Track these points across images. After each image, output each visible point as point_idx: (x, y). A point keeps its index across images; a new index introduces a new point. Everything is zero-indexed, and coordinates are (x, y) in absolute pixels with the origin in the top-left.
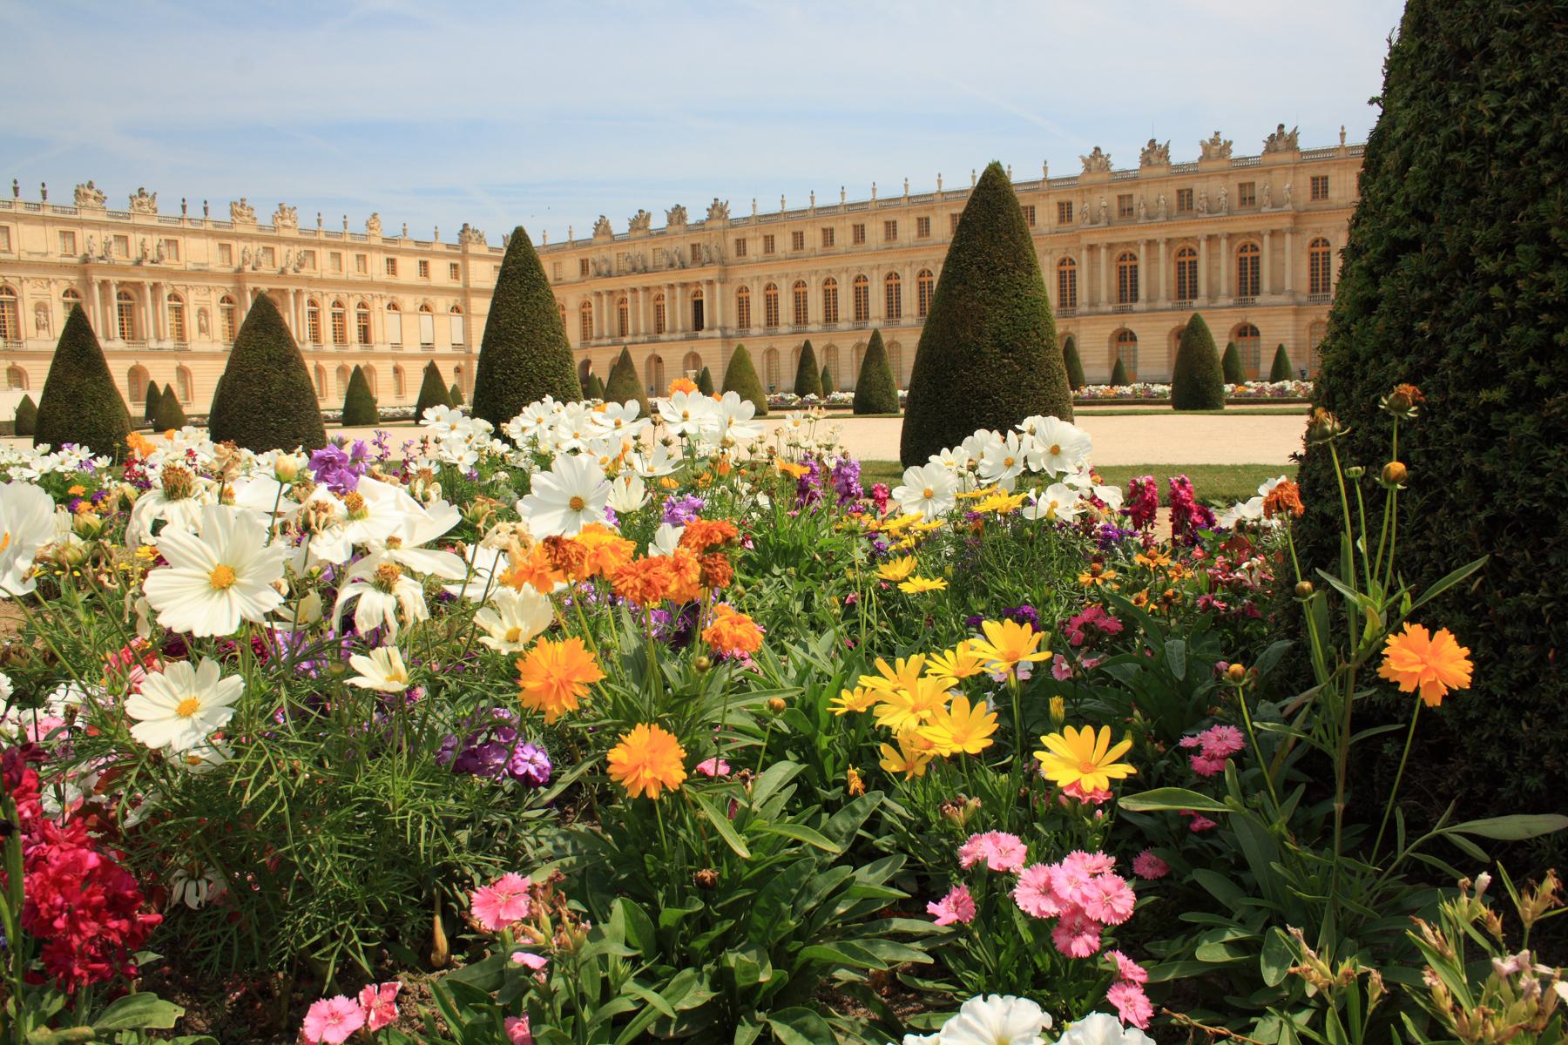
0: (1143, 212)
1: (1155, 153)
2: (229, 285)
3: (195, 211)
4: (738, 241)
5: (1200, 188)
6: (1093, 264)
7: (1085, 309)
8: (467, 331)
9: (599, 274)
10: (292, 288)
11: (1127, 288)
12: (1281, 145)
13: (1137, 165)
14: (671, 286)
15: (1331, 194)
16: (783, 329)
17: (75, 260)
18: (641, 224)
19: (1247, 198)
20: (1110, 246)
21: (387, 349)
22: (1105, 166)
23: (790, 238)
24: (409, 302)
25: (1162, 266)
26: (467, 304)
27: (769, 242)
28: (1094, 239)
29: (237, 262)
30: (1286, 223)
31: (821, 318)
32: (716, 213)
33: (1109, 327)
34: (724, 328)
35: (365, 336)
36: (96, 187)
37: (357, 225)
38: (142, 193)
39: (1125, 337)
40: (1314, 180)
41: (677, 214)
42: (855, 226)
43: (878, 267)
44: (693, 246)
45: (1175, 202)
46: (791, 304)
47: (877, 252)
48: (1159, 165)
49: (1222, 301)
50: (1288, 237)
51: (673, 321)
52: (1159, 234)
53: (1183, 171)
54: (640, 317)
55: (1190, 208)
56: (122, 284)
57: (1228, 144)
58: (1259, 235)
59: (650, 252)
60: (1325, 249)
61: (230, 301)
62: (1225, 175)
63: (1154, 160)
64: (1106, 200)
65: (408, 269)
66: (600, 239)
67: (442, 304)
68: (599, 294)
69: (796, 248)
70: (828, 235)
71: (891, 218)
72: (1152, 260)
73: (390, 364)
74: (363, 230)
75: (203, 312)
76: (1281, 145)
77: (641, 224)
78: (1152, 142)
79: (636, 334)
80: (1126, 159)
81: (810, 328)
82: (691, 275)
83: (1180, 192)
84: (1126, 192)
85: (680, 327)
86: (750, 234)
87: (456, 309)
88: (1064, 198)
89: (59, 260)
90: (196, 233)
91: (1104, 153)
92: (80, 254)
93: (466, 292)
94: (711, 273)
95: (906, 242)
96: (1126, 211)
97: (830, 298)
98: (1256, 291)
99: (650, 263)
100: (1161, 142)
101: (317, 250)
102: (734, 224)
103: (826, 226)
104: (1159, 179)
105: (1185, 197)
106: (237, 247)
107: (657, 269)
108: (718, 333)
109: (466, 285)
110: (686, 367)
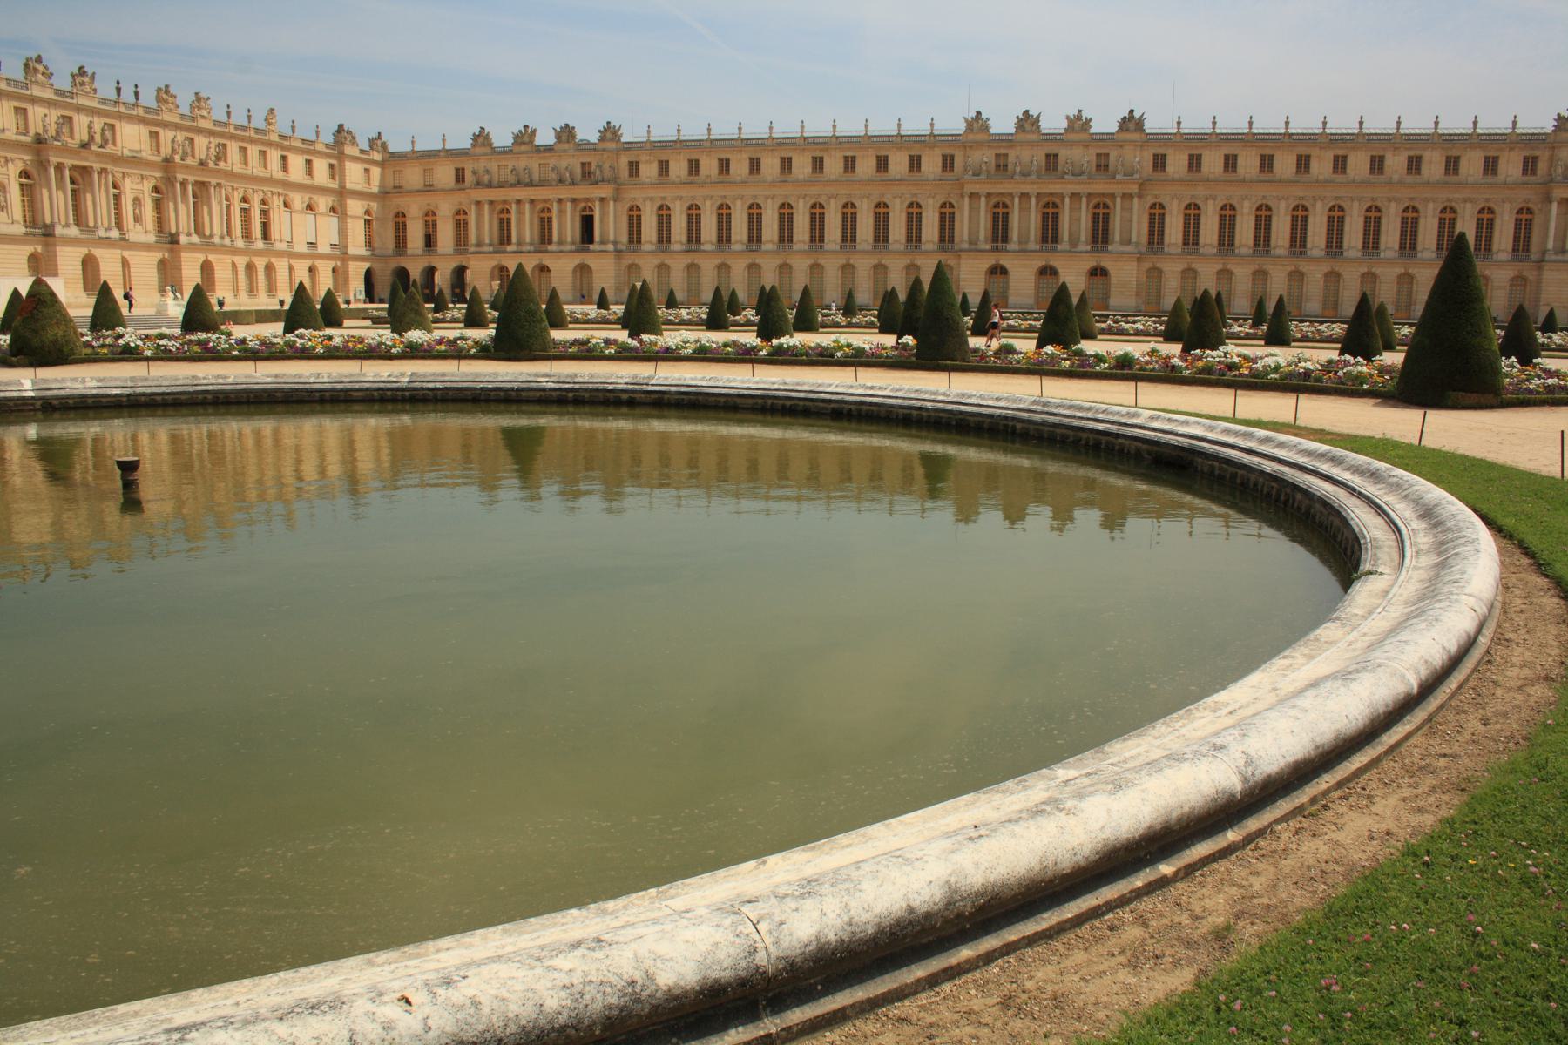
1: (1027, 122)
3: (127, 95)
4: (631, 163)
5: (1064, 153)
6: (974, 210)
7: (966, 246)
8: (343, 232)
9: (478, 184)
11: (1000, 232)
13: (1013, 131)
14: (560, 201)
17: (28, 139)
19: (1102, 165)
20: (988, 195)
22: (985, 127)
23: (685, 165)
24: (298, 200)
27: (664, 167)
28: (976, 188)
29: (166, 150)
30: (1134, 189)
31: (714, 238)
32: (609, 135)
34: (615, 243)
35: (266, 236)
38: (82, 71)
39: (998, 271)
40: (1156, 156)
41: (566, 133)
43: (773, 197)
44: (583, 164)
45: (1043, 164)
46: (684, 224)
48: (1032, 132)
49: (1082, 247)
50: (1136, 200)
53: (1052, 138)
55: (1056, 169)
56: (74, 168)
57: (1088, 121)
58: (1113, 196)
63: (1028, 127)
64: (986, 157)
66: (479, 150)
67: (323, 203)
68: (478, 203)
70: (724, 165)
71: (786, 154)
72: (1024, 210)
73: (307, 263)
74: (262, 125)
75: (137, 202)
76: (1131, 126)
77: (526, 139)
78: (1026, 112)
79: (561, 242)
80: (1002, 124)
82: (582, 192)
83: (1048, 156)
84: (1003, 151)
86: (643, 158)
87: (333, 210)
89: (14, 137)
90: (130, 119)
91: (984, 116)
92: (32, 133)
93: (342, 193)
94: (605, 191)
95: (801, 177)
96: (1001, 166)
98: (1106, 240)
99: (536, 177)
100: (1034, 113)
102: (629, 147)
103: (723, 156)
105: (1052, 159)
106: (166, 136)
107: (542, 184)
108: (611, 247)
109: (342, 186)
110: (492, 279)
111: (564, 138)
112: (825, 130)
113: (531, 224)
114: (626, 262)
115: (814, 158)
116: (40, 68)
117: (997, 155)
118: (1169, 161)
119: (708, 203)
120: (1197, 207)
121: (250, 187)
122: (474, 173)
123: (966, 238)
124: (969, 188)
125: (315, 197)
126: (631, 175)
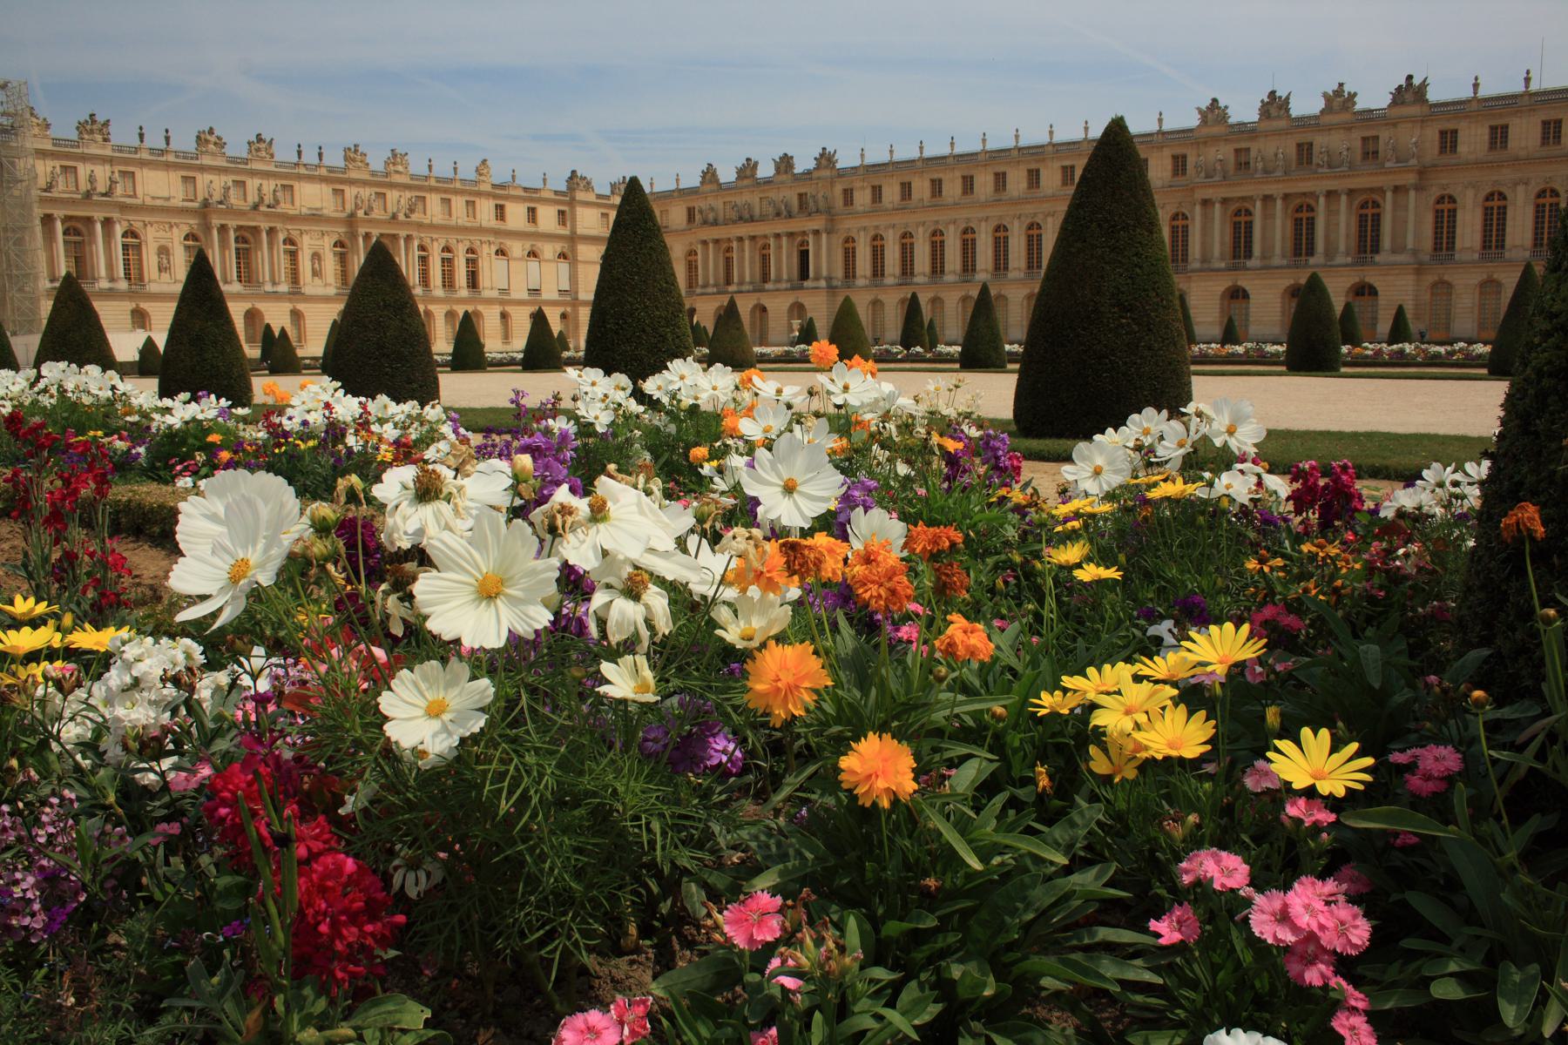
0: (1260, 165)
1: (1275, 105)
2: (342, 230)
3: (310, 157)
4: (845, 191)
5: (1320, 141)
7: (1197, 265)
8: (573, 278)
9: (705, 222)
10: (403, 233)
11: (1241, 244)
12: (1408, 97)
13: (1256, 118)
14: (778, 236)
15: (1460, 148)
16: (889, 280)
17: (196, 205)
18: (748, 173)
19: (1370, 152)
20: (1225, 201)
21: (495, 294)
22: (1223, 117)
23: (897, 189)
25: (1278, 222)
26: (574, 250)
27: (877, 192)
28: (1209, 193)
29: (349, 207)
30: (1411, 179)
31: (927, 269)
32: (824, 162)
33: (1221, 285)
34: (829, 279)
35: (473, 281)
36: (217, 133)
37: (467, 171)
38: (259, 138)
39: (1237, 294)
40: (1443, 133)
41: (785, 163)
42: (964, 178)
44: (800, 195)
45: (1294, 157)
46: (897, 255)
47: (985, 205)
49: (1340, 260)
50: (1412, 194)
51: (779, 270)
52: (1275, 189)
53: (1305, 123)
54: (746, 266)
55: (1310, 162)
56: (239, 228)
57: (1353, 96)
58: (1381, 191)
60: (1451, 206)
61: (342, 246)
62: (1348, 128)
63: (1274, 112)
64: (1223, 153)
65: (516, 215)
66: (708, 188)
67: (549, 250)
68: (705, 243)
69: (903, 199)
70: (937, 186)
71: (1001, 169)
72: (1268, 216)
74: (473, 176)
75: (316, 256)
76: (1408, 97)
77: (748, 173)
78: (1273, 93)
79: (741, 283)
80: (1244, 110)
81: (916, 280)
82: (796, 225)
83: (1299, 146)
84: (1243, 145)
85: (785, 277)
86: (858, 184)
87: (563, 256)
88: (1179, 151)
89: (181, 204)
90: (310, 178)
91: (1222, 104)
92: (200, 198)
93: (573, 239)
94: (817, 223)
96: (1243, 164)
97: (937, 250)
98: (1376, 249)
99: (757, 212)
101: (428, 196)
102: (842, 174)
103: (935, 176)
104: (1278, 133)
107: (763, 218)
108: (823, 283)
109: (573, 232)
110: (791, 317)
111: (783, 168)
112: (1041, 138)
113: (752, 262)
115: (1030, 171)
117: (1237, 151)
118: (1462, 137)
119: (921, 230)
120: (1502, 196)
121: (476, 238)
122: (701, 212)
123: (1198, 256)
124: (1200, 194)
125: (539, 244)
126: (846, 204)
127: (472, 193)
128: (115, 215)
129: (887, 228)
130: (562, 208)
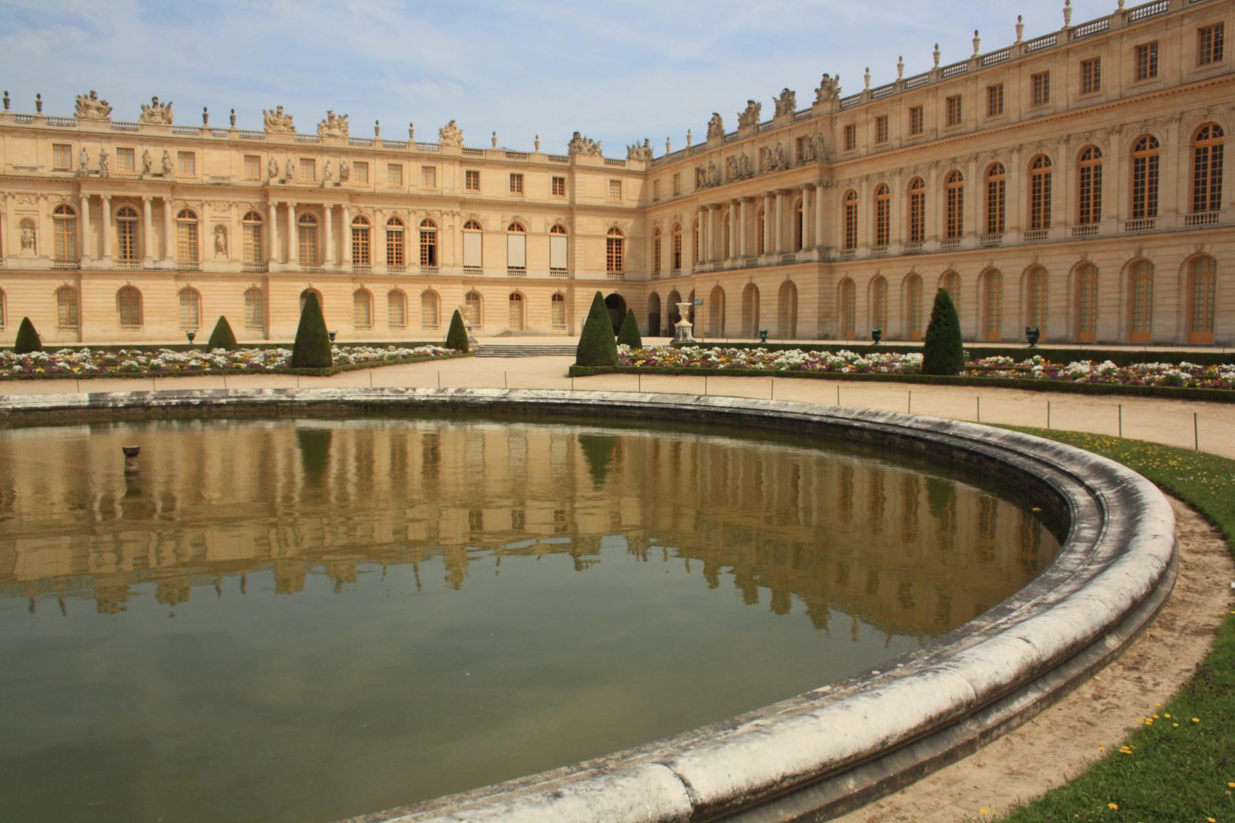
10: (328, 203)
18: (750, 119)
21: (459, 271)
26: (572, 224)
32: (824, 93)
36: (100, 97)
37: (428, 135)
43: (1020, 149)
44: (800, 140)
51: (772, 241)
59: (757, 152)
61: (257, 217)
65: (495, 183)
67: (538, 223)
75: (221, 229)
94: (810, 175)
101: (371, 161)
102: (844, 105)
108: (815, 255)
114: (839, 276)
116: (93, 104)
119: (933, 173)
127: (431, 160)
128: (166, 196)
129: (893, 174)
130: (559, 175)
